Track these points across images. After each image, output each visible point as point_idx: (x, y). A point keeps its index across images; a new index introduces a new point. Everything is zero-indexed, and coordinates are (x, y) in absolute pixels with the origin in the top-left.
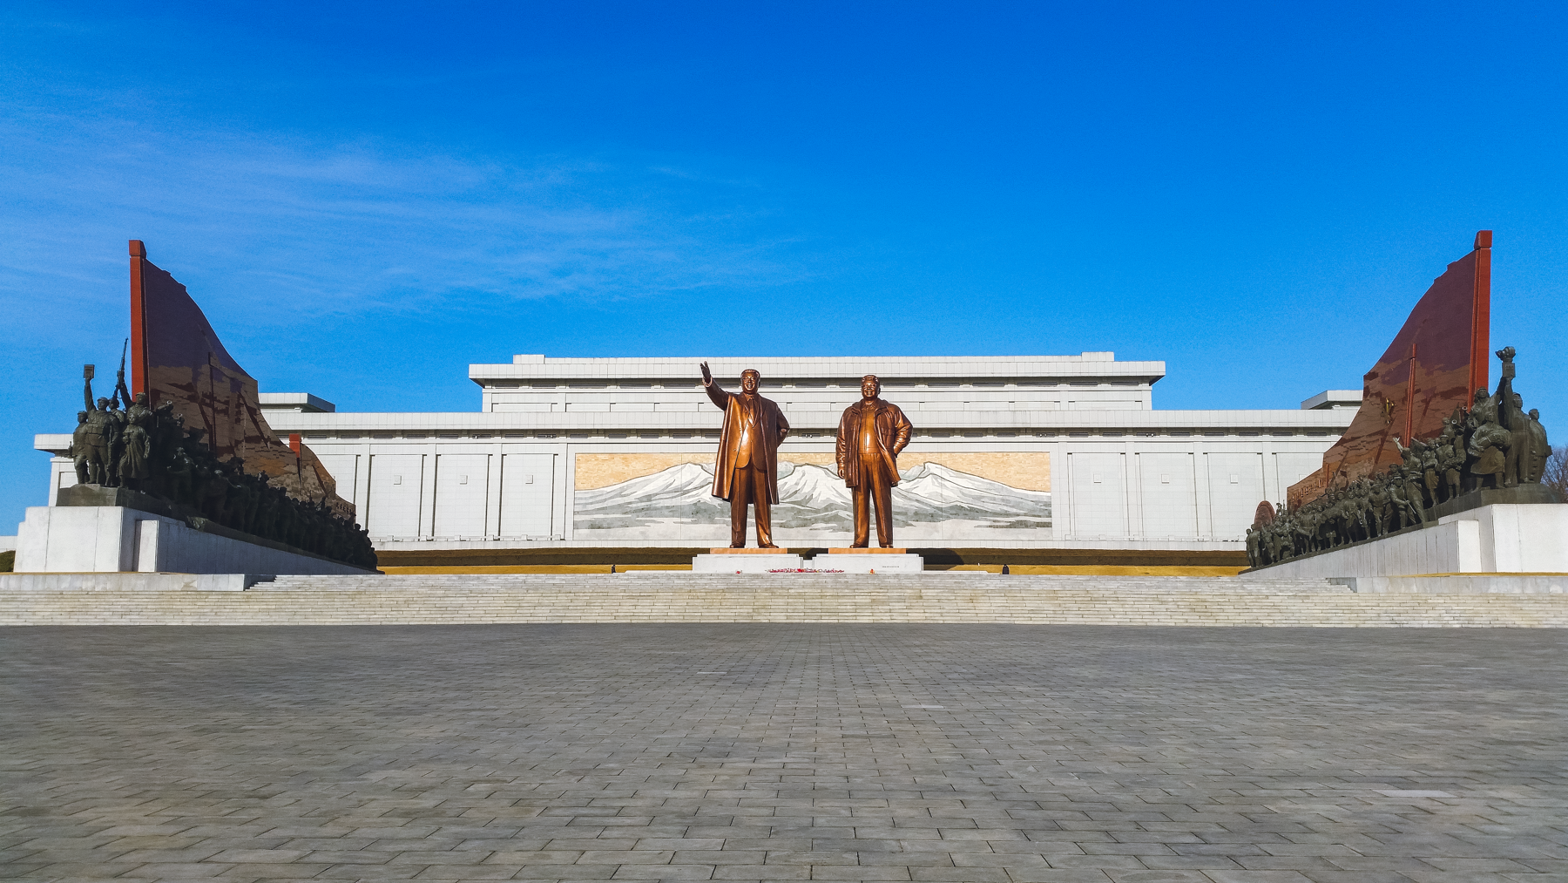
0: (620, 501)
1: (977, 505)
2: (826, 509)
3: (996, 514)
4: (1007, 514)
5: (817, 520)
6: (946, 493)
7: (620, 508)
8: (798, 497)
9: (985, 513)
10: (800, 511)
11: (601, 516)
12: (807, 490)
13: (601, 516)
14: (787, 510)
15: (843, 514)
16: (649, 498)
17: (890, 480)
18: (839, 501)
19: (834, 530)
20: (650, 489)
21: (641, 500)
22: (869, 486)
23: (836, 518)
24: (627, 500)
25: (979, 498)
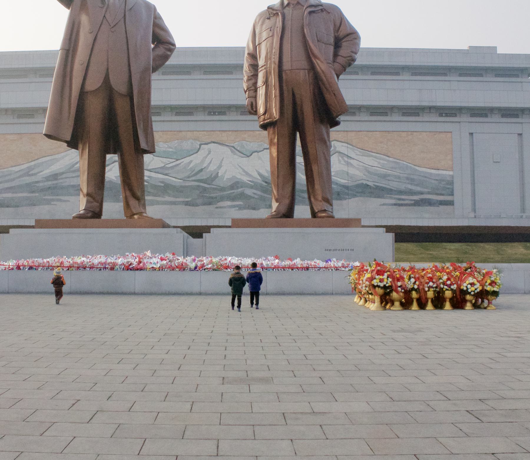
0: (27, 180)
1: (382, 184)
2: (232, 187)
3: (401, 192)
4: (411, 193)
5: (222, 199)
6: (352, 171)
7: (30, 187)
8: (203, 176)
9: (390, 191)
10: (205, 189)
11: (9, 195)
12: (212, 168)
13: (9, 195)
14: (193, 188)
15: (249, 192)
16: (55, 176)
17: (328, 113)
18: (245, 179)
19: (240, 208)
20: (55, 168)
21: (47, 179)
22: (297, 125)
23: (242, 196)
24: (33, 179)
25: (384, 176)
